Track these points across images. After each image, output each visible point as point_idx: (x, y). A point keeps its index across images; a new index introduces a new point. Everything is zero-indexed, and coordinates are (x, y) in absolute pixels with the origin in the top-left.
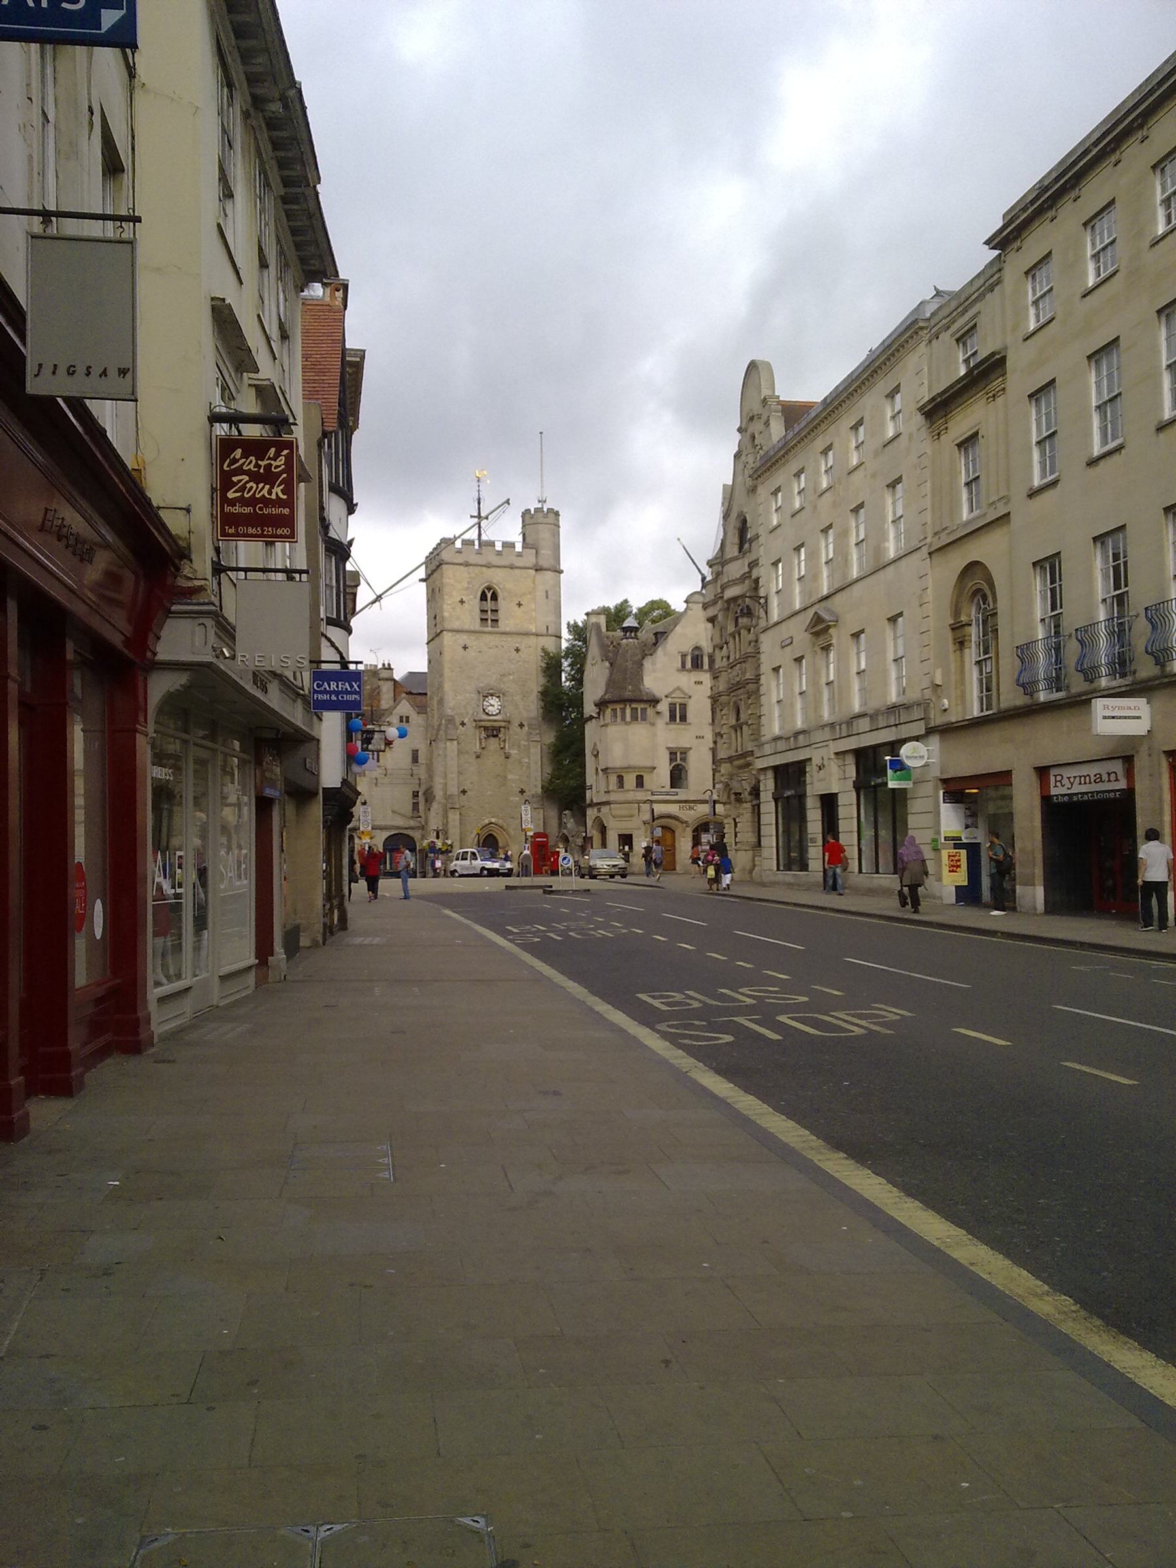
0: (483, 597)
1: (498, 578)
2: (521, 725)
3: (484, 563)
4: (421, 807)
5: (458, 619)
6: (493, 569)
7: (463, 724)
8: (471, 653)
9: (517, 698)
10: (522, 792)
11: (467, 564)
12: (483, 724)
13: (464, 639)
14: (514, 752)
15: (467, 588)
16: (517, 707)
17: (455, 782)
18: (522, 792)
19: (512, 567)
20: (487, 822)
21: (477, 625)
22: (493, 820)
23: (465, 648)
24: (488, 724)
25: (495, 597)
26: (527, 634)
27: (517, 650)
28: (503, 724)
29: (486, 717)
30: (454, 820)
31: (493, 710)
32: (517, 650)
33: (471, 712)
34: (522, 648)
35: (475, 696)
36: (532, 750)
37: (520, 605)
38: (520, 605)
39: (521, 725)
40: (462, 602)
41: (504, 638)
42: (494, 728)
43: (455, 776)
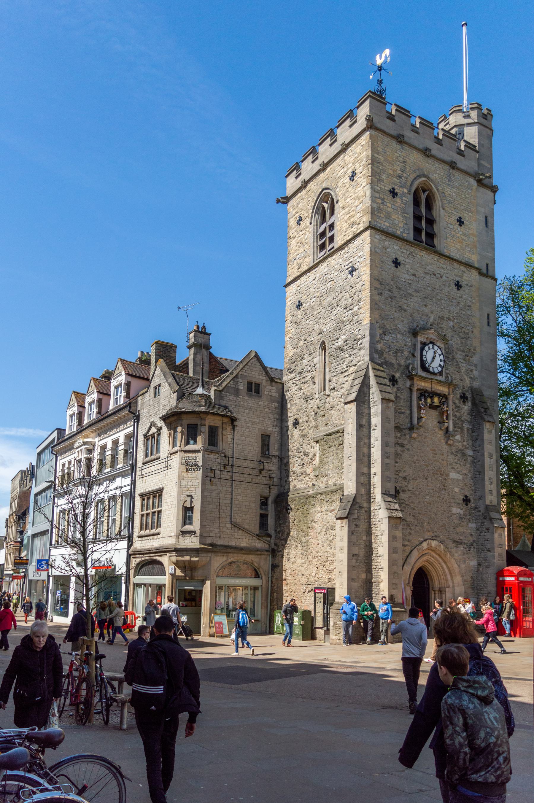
3: (421, 147)
4: (271, 521)
6: (430, 161)
8: (402, 274)
19: (452, 165)
21: (411, 236)
23: (396, 263)
26: (468, 265)
27: (458, 286)
28: (444, 390)
29: (424, 374)
31: (436, 365)
32: (458, 286)
34: (463, 284)
35: (409, 341)
36: (487, 436)
37: (460, 222)
38: (460, 222)
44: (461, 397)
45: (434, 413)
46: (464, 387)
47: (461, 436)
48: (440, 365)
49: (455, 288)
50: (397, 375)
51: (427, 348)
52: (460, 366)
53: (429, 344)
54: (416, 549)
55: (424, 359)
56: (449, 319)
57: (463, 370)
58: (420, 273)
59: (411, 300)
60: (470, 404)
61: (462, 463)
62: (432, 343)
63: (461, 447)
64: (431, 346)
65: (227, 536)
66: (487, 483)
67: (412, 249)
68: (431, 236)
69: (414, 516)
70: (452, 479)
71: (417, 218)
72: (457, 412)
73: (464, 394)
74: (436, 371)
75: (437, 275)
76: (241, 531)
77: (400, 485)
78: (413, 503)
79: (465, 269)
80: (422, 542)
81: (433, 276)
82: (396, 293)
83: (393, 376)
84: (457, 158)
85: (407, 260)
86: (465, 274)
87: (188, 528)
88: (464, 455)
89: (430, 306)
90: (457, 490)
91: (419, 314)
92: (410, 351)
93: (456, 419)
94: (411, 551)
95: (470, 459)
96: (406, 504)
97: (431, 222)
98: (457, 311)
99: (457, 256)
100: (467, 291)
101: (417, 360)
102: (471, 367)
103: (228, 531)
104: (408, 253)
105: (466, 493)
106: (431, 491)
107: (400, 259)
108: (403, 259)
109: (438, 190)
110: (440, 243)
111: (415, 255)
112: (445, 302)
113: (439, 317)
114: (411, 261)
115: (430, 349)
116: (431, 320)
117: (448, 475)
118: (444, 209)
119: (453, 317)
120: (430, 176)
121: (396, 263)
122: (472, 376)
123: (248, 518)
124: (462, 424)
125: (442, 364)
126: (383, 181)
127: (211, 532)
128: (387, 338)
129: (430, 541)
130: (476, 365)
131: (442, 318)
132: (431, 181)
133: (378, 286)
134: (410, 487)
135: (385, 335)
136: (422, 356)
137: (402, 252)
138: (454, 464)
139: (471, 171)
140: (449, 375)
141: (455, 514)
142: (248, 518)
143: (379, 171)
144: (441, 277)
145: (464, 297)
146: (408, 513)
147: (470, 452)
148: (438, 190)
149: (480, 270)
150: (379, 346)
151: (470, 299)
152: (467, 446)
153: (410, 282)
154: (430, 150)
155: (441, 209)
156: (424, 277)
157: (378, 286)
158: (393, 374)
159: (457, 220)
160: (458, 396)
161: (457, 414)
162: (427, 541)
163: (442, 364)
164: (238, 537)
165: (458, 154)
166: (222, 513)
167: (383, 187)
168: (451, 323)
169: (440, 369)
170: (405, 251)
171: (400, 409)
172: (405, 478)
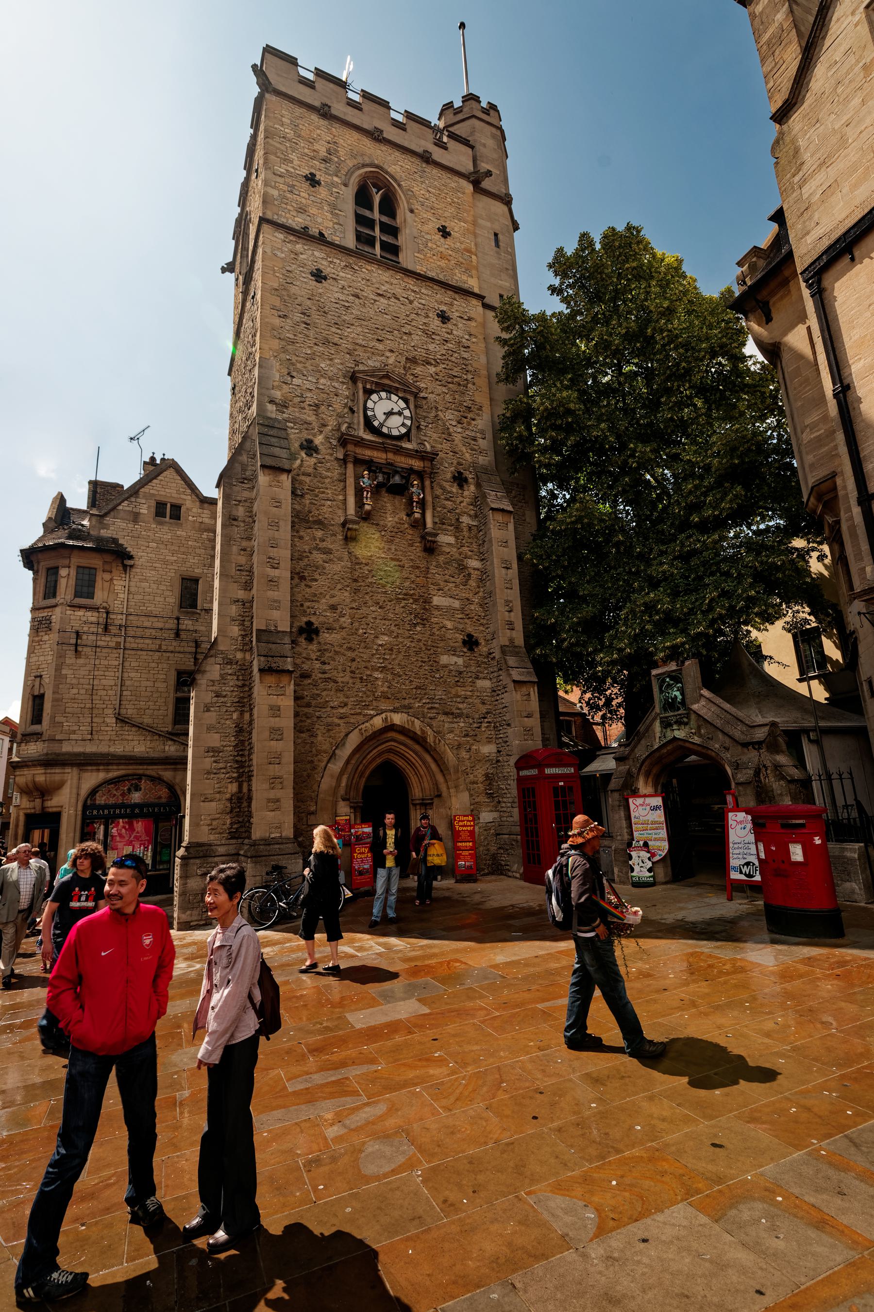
0: (362, 198)
1: (397, 166)
2: (460, 480)
5: (302, 210)
7: (309, 447)
8: (331, 293)
9: (450, 417)
10: (471, 643)
11: (324, 112)
12: (368, 453)
13: (313, 256)
14: (446, 539)
15: (325, 160)
16: (447, 435)
17: (283, 594)
18: (471, 643)
19: (426, 158)
20: (378, 722)
21: (350, 241)
22: (397, 719)
23: (319, 276)
24: (379, 457)
25: (389, 206)
27: (444, 317)
28: (417, 464)
30: (275, 711)
31: (395, 425)
33: (332, 423)
34: (455, 315)
36: (495, 533)
37: (445, 233)
38: (445, 233)
39: (460, 480)
40: (312, 181)
41: (411, 283)
42: (390, 469)
43: (284, 574)
44: (454, 478)
45: (400, 502)
46: (459, 464)
47: (457, 538)
48: (403, 425)
49: (437, 322)
50: (318, 440)
51: (374, 397)
52: (451, 430)
53: (379, 392)
54: (357, 730)
55: (370, 413)
56: (429, 363)
57: (458, 438)
58: (369, 293)
59: (349, 330)
60: (472, 488)
61: (458, 581)
62: (389, 392)
63: (457, 556)
64: (383, 394)
65: (107, 738)
66: (501, 608)
67: (351, 260)
68: (393, 250)
69: (352, 672)
70: (438, 608)
71: (360, 220)
72: (447, 499)
73: (460, 473)
74: (395, 433)
75: (401, 299)
76: (134, 729)
77: (321, 619)
78: (350, 649)
79: (457, 296)
80: (373, 716)
81: (393, 300)
82: (316, 317)
83: (310, 441)
84: (432, 148)
85: (341, 274)
86: (455, 302)
87: (36, 728)
88: (462, 568)
89: (388, 342)
90: (449, 625)
91: (365, 352)
92: (346, 404)
93: (445, 510)
94: (347, 735)
95: (475, 575)
96: (336, 653)
97: (394, 231)
98: (444, 352)
99: (441, 277)
100: (460, 325)
101: (359, 416)
102: (473, 434)
103: (107, 729)
104: (343, 264)
105: (470, 629)
106: (393, 628)
107: (327, 270)
108: (333, 271)
109: (399, 185)
110: (406, 259)
111: (357, 268)
112: (418, 338)
113: (407, 359)
114: (349, 276)
115: (381, 399)
116: (391, 361)
117: (427, 601)
118: (412, 211)
119: (435, 360)
120: (386, 167)
121: (319, 276)
122: (476, 447)
123: (151, 707)
124: (458, 520)
125: (408, 422)
126: (292, 162)
127: (74, 732)
128: (296, 381)
129: (389, 714)
130: (482, 432)
131: (413, 361)
132: (387, 173)
133: (277, 303)
134: (345, 621)
135: (293, 377)
136: (365, 409)
137: (331, 262)
138: (442, 583)
139: (463, 170)
140: (426, 443)
141: (445, 666)
142: (151, 707)
143: (283, 148)
144: (411, 302)
145: (455, 332)
146: (340, 667)
147: (474, 563)
148: (399, 185)
149: (484, 297)
150: (278, 394)
151: (467, 337)
152: (470, 553)
153: (347, 304)
154: (382, 131)
155: (407, 212)
156: (375, 301)
157: (277, 303)
158: (310, 437)
159: (439, 229)
160: (449, 476)
161: (449, 504)
162: (384, 716)
163: (408, 422)
164: (130, 738)
165: (436, 144)
166: (98, 702)
167: (292, 170)
168: (432, 370)
169: (403, 430)
170: (335, 260)
171: (323, 493)
172: (333, 608)
